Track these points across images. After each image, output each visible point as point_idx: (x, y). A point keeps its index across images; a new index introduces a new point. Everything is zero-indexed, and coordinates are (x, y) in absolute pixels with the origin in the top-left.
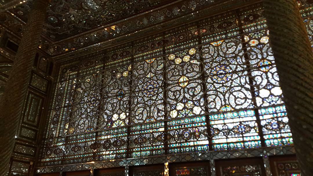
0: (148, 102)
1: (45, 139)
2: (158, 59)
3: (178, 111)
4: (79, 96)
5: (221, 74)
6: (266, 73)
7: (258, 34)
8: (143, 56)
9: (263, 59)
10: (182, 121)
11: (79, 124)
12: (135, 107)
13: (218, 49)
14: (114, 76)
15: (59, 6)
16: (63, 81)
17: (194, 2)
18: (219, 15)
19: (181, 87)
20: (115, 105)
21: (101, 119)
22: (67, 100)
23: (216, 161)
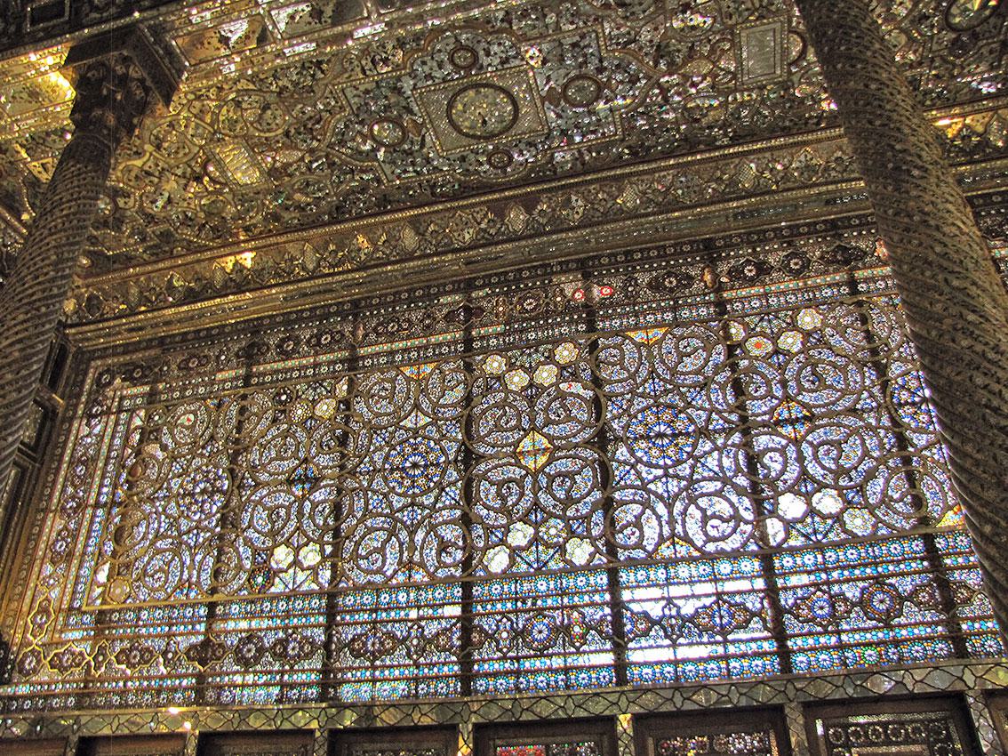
0: (406, 513)
2: (445, 367)
3: (515, 552)
4: (153, 473)
5: (660, 435)
6: (796, 442)
7: (769, 321)
8: (392, 353)
9: (787, 398)
10: (526, 586)
11: (146, 570)
12: (357, 525)
13: (650, 353)
14: (283, 412)
15: (129, 163)
16: (95, 416)
17: (577, 201)
18: (653, 248)
19: (525, 468)
20: (283, 512)
21: (229, 559)
22: (107, 481)
23: (637, 719)
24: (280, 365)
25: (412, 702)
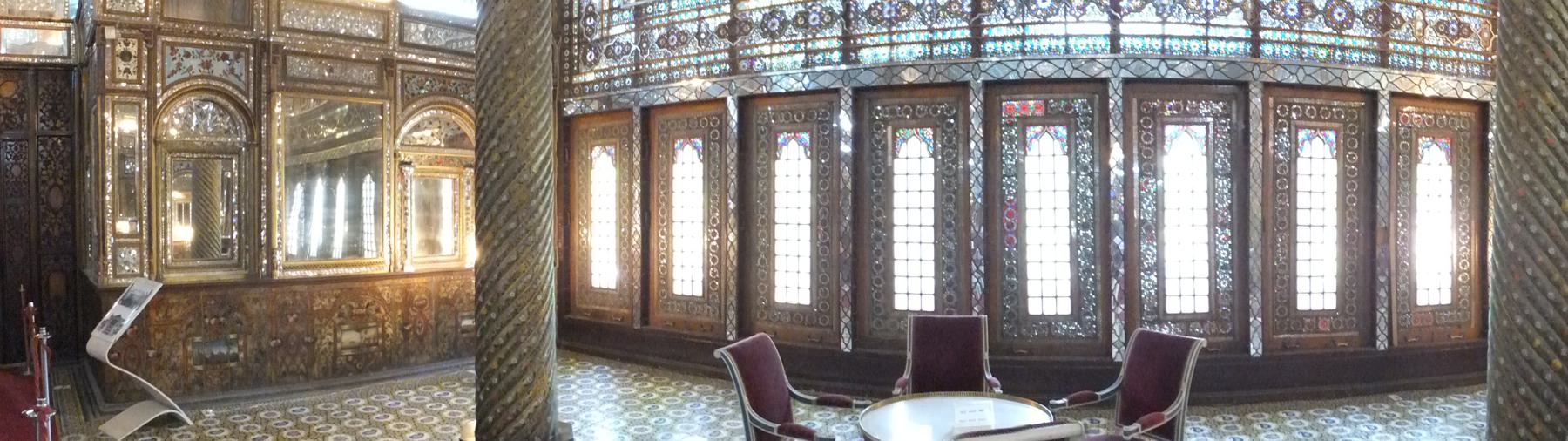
1: (571, 20)
25: (928, 59)
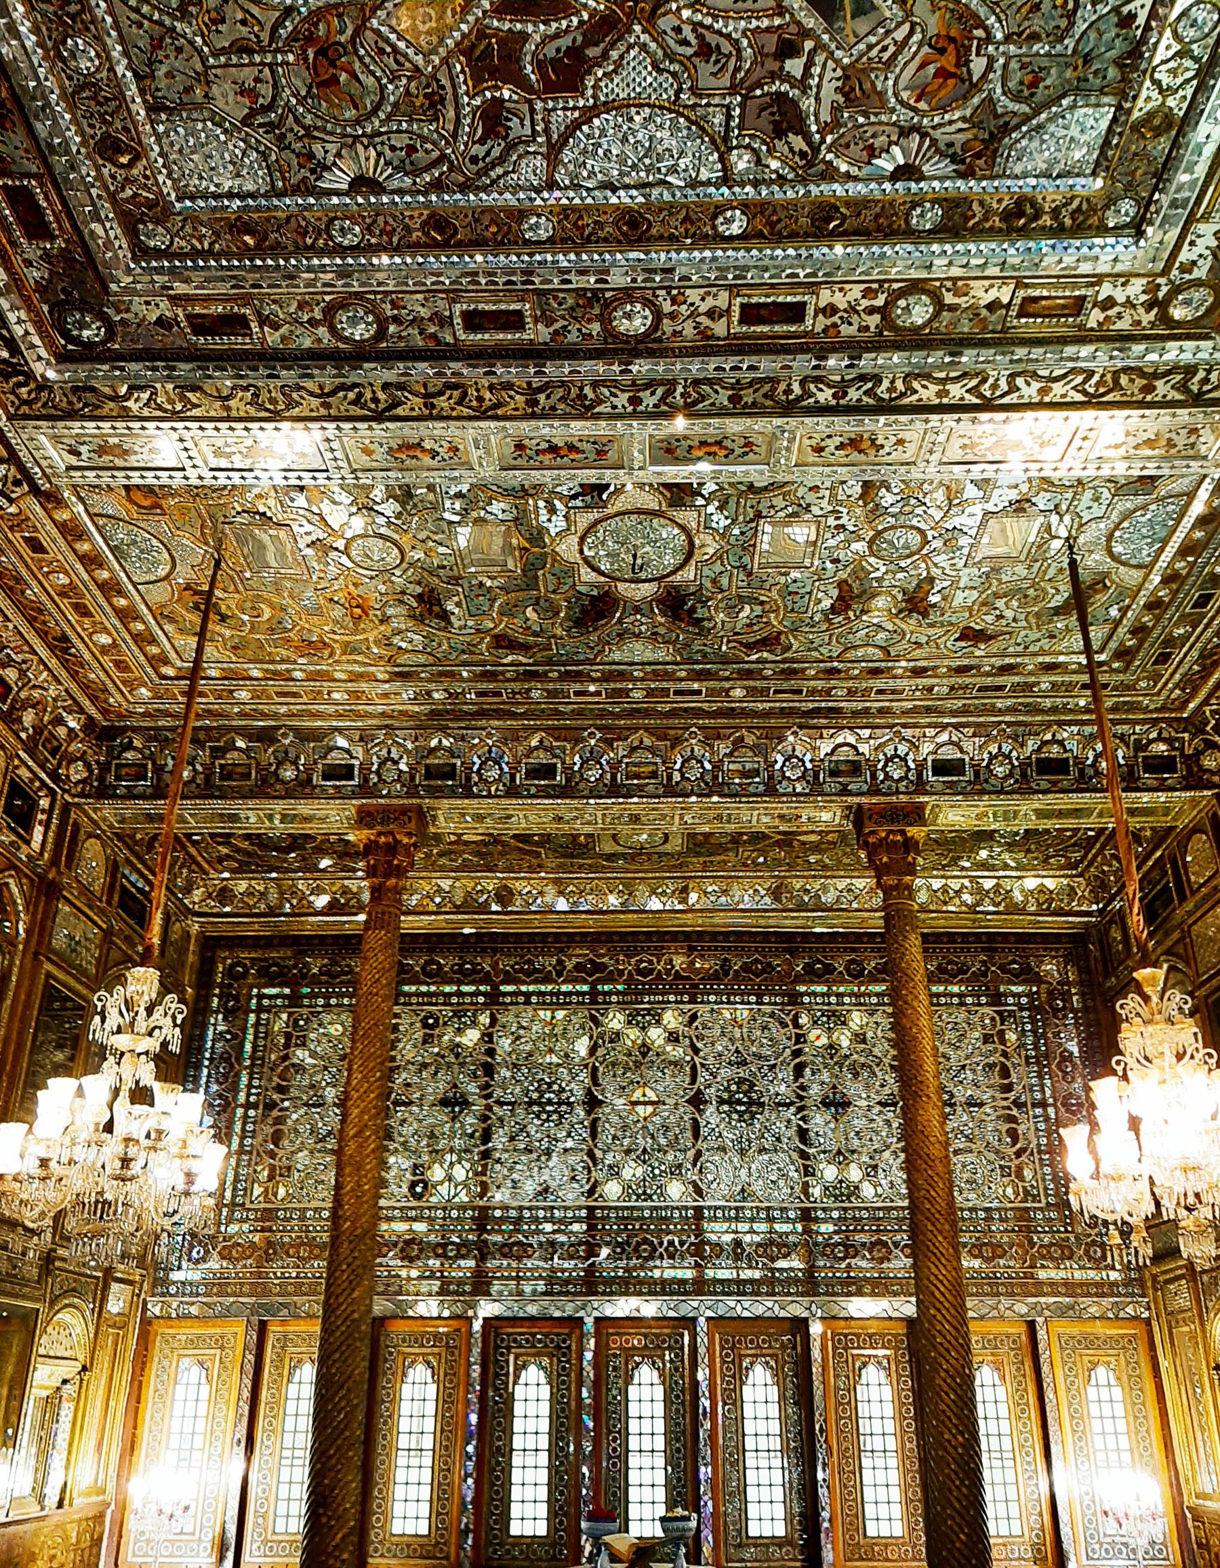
5: (739, 1102)
24: (424, 988)
